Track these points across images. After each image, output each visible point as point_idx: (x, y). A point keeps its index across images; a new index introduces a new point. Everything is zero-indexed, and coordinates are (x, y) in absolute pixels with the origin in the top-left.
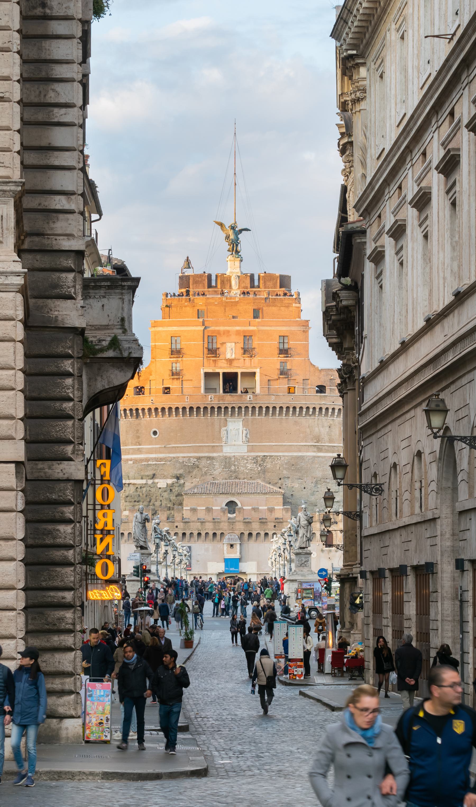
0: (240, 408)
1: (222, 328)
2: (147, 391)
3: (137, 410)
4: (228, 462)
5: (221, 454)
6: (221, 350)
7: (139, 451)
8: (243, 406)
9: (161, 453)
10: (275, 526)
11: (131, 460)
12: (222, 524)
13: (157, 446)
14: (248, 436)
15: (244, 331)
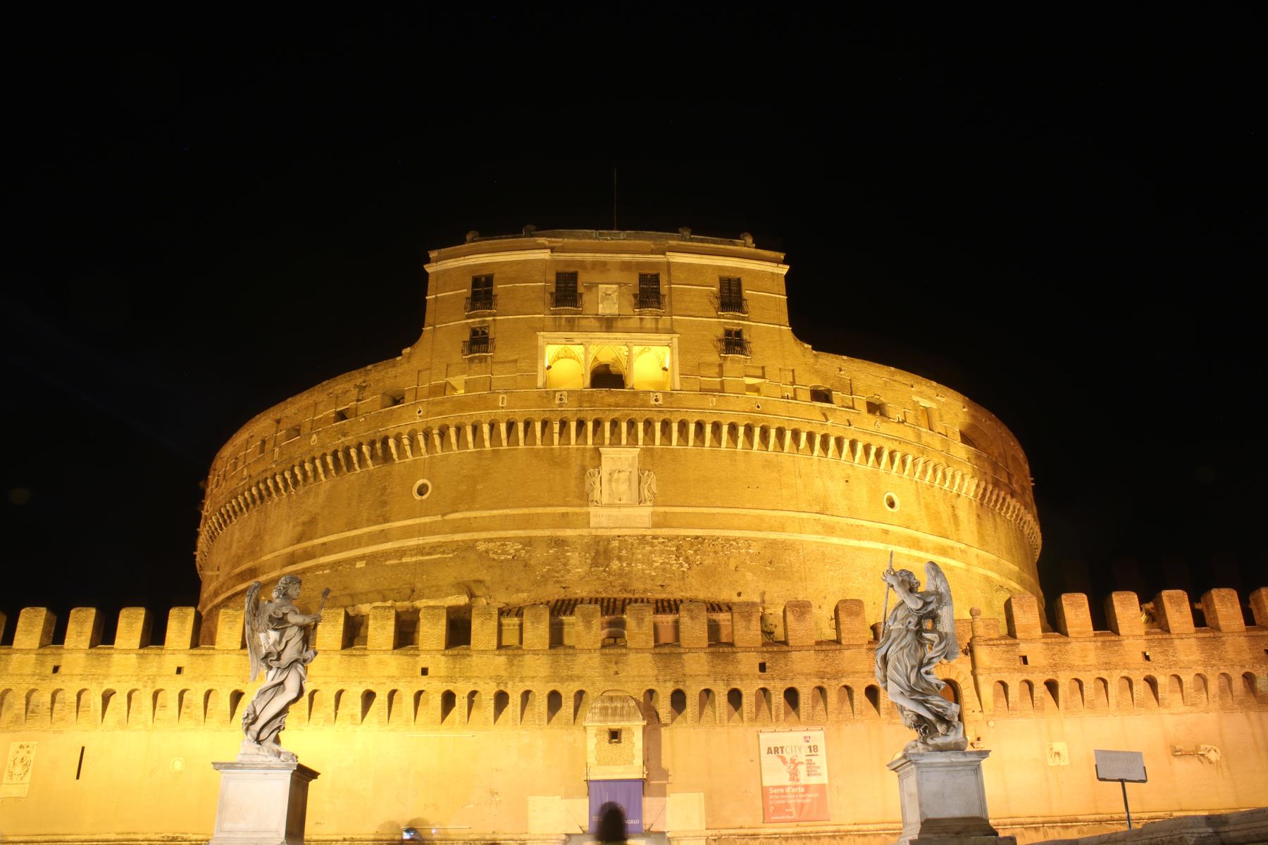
0: (632, 424)
1: (588, 257)
2: (409, 398)
3: (385, 442)
4: (601, 551)
5: (585, 532)
6: (587, 298)
7: (384, 536)
8: (639, 415)
9: (434, 533)
10: (763, 667)
11: (362, 558)
12: (583, 658)
13: (427, 520)
14: (654, 487)
15: (639, 264)
